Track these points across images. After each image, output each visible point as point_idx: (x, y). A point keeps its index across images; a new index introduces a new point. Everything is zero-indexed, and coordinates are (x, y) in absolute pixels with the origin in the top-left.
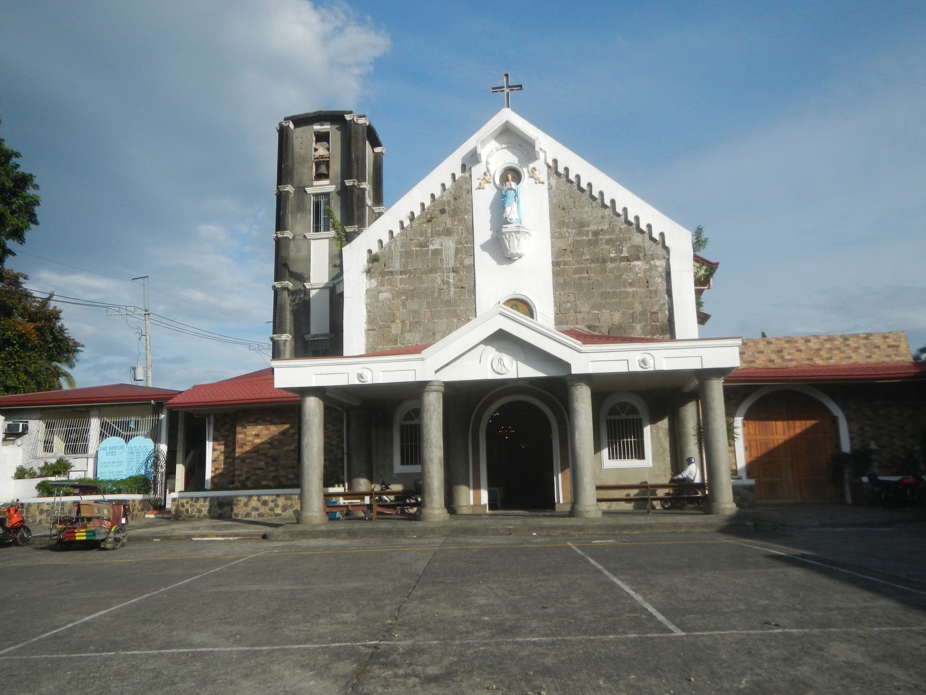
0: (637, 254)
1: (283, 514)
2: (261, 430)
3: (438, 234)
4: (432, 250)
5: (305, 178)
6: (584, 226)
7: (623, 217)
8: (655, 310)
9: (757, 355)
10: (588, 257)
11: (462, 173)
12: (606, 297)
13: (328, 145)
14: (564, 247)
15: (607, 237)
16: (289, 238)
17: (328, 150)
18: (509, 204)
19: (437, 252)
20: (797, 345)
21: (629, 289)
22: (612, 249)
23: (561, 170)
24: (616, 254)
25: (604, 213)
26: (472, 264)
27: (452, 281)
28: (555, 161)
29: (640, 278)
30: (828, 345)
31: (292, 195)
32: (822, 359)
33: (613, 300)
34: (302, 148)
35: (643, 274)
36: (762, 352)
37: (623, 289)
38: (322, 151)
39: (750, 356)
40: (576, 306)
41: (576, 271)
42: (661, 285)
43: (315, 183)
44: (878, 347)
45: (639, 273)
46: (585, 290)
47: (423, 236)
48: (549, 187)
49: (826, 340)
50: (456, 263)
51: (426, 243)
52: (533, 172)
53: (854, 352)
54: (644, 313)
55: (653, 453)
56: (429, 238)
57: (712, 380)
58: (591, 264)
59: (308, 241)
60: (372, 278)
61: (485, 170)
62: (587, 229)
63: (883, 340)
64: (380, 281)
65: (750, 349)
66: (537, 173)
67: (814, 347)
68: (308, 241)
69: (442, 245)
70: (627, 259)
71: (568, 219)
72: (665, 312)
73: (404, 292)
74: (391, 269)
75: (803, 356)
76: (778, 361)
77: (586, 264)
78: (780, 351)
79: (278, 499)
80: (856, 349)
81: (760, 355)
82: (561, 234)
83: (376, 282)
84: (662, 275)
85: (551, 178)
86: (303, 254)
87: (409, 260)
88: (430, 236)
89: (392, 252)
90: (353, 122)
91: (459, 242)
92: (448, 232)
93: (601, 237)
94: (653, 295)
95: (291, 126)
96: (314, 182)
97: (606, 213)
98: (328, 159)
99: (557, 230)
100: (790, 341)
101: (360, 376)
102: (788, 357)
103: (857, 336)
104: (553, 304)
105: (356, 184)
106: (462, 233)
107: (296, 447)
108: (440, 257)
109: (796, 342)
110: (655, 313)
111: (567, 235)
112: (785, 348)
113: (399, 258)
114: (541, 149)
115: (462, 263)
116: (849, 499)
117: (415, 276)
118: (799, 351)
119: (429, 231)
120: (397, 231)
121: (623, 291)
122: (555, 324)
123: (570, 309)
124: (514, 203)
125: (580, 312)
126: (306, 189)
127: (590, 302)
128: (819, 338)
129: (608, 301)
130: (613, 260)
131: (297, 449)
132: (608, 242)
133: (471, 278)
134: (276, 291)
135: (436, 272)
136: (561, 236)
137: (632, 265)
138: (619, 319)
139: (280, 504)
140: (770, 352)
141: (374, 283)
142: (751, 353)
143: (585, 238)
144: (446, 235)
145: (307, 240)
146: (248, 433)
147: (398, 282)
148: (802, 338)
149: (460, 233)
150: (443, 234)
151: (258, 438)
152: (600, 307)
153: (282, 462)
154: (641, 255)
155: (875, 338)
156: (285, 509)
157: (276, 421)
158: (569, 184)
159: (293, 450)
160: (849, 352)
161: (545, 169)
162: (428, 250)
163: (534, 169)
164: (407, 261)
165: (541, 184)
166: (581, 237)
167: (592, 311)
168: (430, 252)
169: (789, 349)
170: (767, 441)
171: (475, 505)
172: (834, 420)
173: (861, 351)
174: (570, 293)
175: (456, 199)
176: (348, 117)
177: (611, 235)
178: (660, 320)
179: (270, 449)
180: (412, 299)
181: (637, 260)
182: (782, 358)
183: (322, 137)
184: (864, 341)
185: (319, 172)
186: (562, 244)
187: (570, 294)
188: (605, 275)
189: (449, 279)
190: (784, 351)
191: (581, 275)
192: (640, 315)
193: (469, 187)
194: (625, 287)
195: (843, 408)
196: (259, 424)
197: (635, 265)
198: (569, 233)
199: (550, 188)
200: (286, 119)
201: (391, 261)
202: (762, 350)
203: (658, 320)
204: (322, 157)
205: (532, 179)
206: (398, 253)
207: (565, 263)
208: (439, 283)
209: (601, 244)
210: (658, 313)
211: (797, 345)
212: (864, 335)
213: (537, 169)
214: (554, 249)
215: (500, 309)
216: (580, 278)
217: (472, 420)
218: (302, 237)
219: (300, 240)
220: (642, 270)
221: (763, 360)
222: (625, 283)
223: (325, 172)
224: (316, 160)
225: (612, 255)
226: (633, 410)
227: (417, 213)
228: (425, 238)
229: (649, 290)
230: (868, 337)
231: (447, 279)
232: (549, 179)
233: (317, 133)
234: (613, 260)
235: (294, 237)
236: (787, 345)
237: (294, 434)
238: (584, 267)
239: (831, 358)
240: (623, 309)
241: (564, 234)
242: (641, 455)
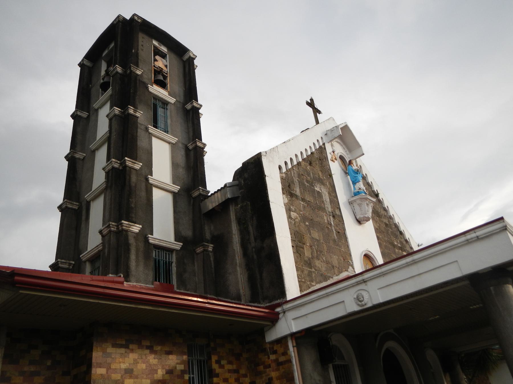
2: (136, 362)
145: (148, 133)
146: (113, 366)
185: (155, 79)
196: (132, 351)
218: (143, 127)
219: (141, 129)
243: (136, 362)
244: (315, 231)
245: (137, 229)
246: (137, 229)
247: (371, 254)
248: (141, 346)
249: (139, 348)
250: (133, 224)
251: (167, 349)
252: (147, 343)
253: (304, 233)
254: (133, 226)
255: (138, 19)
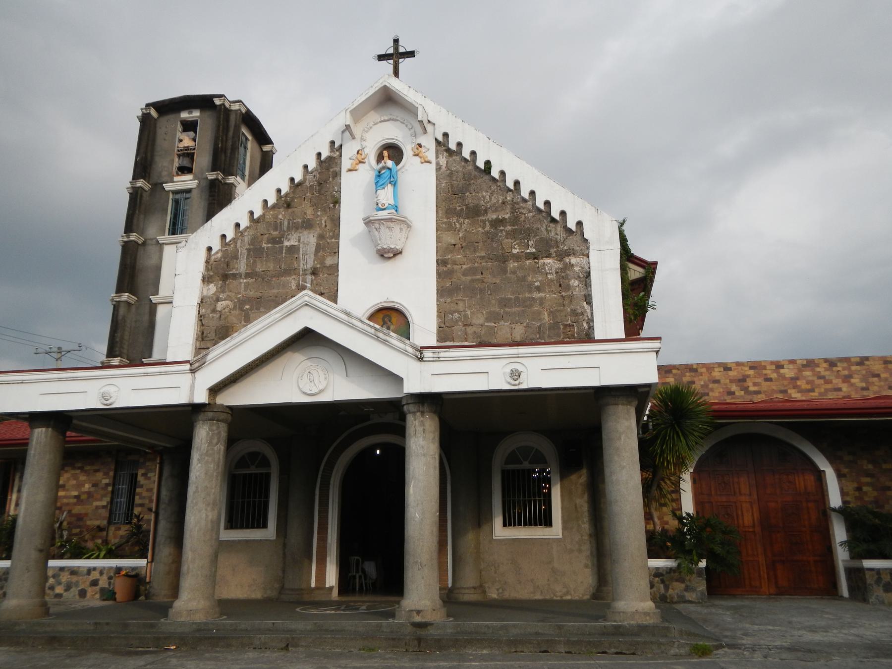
0: (545, 248)
1: (65, 594)
3: (295, 227)
4: (287, 246)
5: (164, 173)
6: (479, 216)
7: (530, 203)
8: (570, 322)
9: (711, 386)
10: (483, 254)
11: (331, 152)
12: (505, 306)
13: (194, 135)
14: (453, 242)
15: (509, 228)
16: (136, 242)
17: (195, 141)
18: (382, 187)
19: (293, 250)
20: (764, 372)
21: (536, 295)
22: (515, 243)
23: (453, 146)
24: (519, 249)
25: (506, 198)
26: (335, 264)
27: (310, 286)
28: (446, 135)
29: (552, 281)
30: (807, 373)
31: (148, 193)
32: (801, 391)
33: (514, 310)
34: (165, 140)
35: (555, 275)
36: (717, 381)
37: (527, 295)
38: (187, 141)
39: (702, 386)
40: (466, 316)
41: (465, 274)
42: (577, 289)
43: (176, 179)
44: (878, 376)
45: (550, 273)
46: (478, 297)
47: (275, 229)
48: (438, 167)
49: (804, 366)
50: (316, 262)
51: (280, 238)
52: (417, 149)
53: (844, 382)
54: (554, 326)
55: (563, 517)
56: (285, 231)
57: (617, 404)
58: (487, 262)
59: (160, 247)
60: (211, 283)
61: (359, 148)
62: (484, 218)
63: (883, 366)
64: (219, 286)
65: (700, 377)
66: (423, 150)
67: (787, 376)
68: (160, 247)
69: (299, 241)
70: (535, 257)
71: (460, 206)
72: (583, 325)
73: (248, 300)
74: (234, 271)
75: (774, 386)
76: (740, 393)
77: (481, 263)
78: (742, 381)
79: (62, 574)
80: (847, 379)
81: (716, 385)
82: (450, 224)
83: (215, 287)
84: (579, 277)
85: (441, 156)
86: (153, 262)
87: (257, 259)
88: (285, 229)
89: (238, 250)
90: (223, 107)
91: (321, 237)
92: (308, 225)
93: (502, 228)
94: (567, 302)
95: (154, 113)
96: (175, 178)
97: (508, 198)
98: (193, 151)
99: (445, 220)
100: (755, 366)
101: (104, 397)
102: (752, 389)
103: (847, 360)
104: (435, 313)
105: (220, 178)
106: (326, 226)
107: (108, 502)
108: (296, 256)
109: (765, 368)
110: (569, 325)
111: (458, 226)
112: (748, 376)
113: (245, 258)
114: (429, 122)
115: (322, 262)
116: (845, 592)
117: (263, 279)
118: (770, 380)
119: (286, 223)
120: (244, 223)
121: (529, 298)
122: (438, 341)
123: (457, 321)
124: (390, 185)
125: (470, 325)
126: (164, 185)
127: (484, 312)
128: (796, 363)
129: (507, 310)
130: (517, 258)
131: (109, 506)
132: (509, 235)
133: (333, 282)
134: (116, 307)
135: (289, 274)
136: (450, 228)
137: (540, 264)
138: (522, 334)
139: (63, 581)
140: (728, 381)
141: (212, 288)
142: (702, 383)
143: (480, 229)
144: (306, 228)
145: (159, 245)
147: (242, 286)
148: (772, 363)
149: (323, 226)
150: (302, 227)
151: (64, 490)
152: (495, 317)
153: (89, 523)
154: (552, 251)
155: (872, 363)
156: (68, 588)
157: (88, 468)
158: (463, 163)
159: (104, 507)
160: (837, 382)
161: (432, 146)
162: (282, 247)
163: (420, 145)
164: (255, 262)
165: (428, 164)
166: (476, 229)
167: (486, 324)
168: (284, 249)
169: (755, 377)
170: (725, 504)
171: (317, 588)
172: (820, 476)
173: (853, 381)
174: (459, 300)
175: (321, 184)
176: (217, 102)
177: (514, 226)
178: (576, 335)
179: (75, 504)
180: (258, 309)
181: (547, 257)
182: (746, 389)
183: (189, 126)
184: (858, 368)
186: (450, 239)
187: (458, 302)
188: (504, 277)
189: (306, 283)
190: (747, 379)
191: (474, 277)
192: (549, 329)
193: (337, 169)
194: (530, 292)
195: (832, 460)
196: (67, 472)
197: (544, 263)
198: (461, 224)
199: (438, 168)
200: (148, 105)
201: (235, 261)
202: (717, 378)
203: (573, 336)
204: (187, 148)
205: (417, 157)
206: (246, 251)
207: (455, 263)
208: (293, 288)
209: (501, 236)
210: (573, 325)
211: (764, 372)
212: (858, 360)
213: (422, 145)
214: (440, 244)
215: (306, 298)
216: (473, 281)
217: (322, 468)
219: (152, 245)
220: (554, 270)
221: (720, 392)
222: (531, 288)
223: (188, 165)
224: (179, 153)
225: (515, 251)
226: (540, 459)
227: (272, 201)
228: (279, 233)
229: (562, 296)
230: (863, 361)
231: (303, 283)
232: (437, 157)
233: (184, 123)
234: (517, 258)
235: (144, 243)
236: (751, 372)
237: (107, 485)
238: (478, 267)
239: (812, 390)
240: (527, 321)
241: (454, 226)
242: (547, 522)
243: (68, 479)
244: (261, 312)
245: (116, 362)
246: (116, 362)
247: (399, 305)
248: (74, 468)
249: (72, 469)
250: (112, 359)
251: (95, 468)
252: (79, 465)
253: (235, 324)
254: (112, 360)
255: (146, 111)
